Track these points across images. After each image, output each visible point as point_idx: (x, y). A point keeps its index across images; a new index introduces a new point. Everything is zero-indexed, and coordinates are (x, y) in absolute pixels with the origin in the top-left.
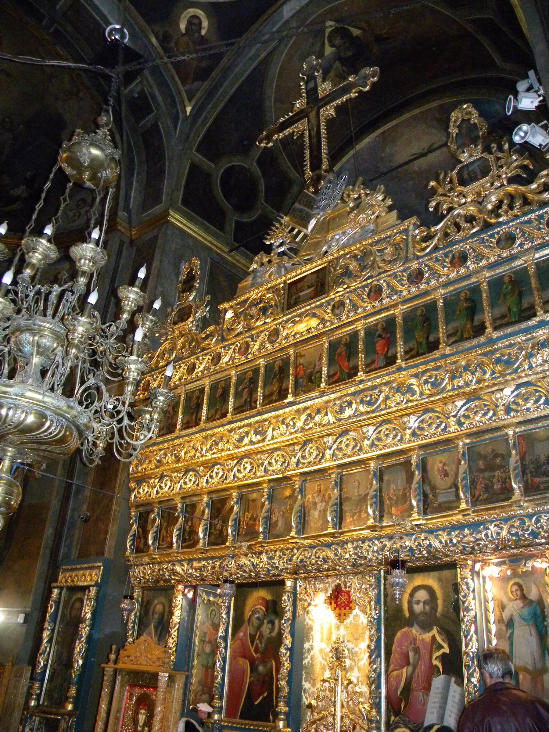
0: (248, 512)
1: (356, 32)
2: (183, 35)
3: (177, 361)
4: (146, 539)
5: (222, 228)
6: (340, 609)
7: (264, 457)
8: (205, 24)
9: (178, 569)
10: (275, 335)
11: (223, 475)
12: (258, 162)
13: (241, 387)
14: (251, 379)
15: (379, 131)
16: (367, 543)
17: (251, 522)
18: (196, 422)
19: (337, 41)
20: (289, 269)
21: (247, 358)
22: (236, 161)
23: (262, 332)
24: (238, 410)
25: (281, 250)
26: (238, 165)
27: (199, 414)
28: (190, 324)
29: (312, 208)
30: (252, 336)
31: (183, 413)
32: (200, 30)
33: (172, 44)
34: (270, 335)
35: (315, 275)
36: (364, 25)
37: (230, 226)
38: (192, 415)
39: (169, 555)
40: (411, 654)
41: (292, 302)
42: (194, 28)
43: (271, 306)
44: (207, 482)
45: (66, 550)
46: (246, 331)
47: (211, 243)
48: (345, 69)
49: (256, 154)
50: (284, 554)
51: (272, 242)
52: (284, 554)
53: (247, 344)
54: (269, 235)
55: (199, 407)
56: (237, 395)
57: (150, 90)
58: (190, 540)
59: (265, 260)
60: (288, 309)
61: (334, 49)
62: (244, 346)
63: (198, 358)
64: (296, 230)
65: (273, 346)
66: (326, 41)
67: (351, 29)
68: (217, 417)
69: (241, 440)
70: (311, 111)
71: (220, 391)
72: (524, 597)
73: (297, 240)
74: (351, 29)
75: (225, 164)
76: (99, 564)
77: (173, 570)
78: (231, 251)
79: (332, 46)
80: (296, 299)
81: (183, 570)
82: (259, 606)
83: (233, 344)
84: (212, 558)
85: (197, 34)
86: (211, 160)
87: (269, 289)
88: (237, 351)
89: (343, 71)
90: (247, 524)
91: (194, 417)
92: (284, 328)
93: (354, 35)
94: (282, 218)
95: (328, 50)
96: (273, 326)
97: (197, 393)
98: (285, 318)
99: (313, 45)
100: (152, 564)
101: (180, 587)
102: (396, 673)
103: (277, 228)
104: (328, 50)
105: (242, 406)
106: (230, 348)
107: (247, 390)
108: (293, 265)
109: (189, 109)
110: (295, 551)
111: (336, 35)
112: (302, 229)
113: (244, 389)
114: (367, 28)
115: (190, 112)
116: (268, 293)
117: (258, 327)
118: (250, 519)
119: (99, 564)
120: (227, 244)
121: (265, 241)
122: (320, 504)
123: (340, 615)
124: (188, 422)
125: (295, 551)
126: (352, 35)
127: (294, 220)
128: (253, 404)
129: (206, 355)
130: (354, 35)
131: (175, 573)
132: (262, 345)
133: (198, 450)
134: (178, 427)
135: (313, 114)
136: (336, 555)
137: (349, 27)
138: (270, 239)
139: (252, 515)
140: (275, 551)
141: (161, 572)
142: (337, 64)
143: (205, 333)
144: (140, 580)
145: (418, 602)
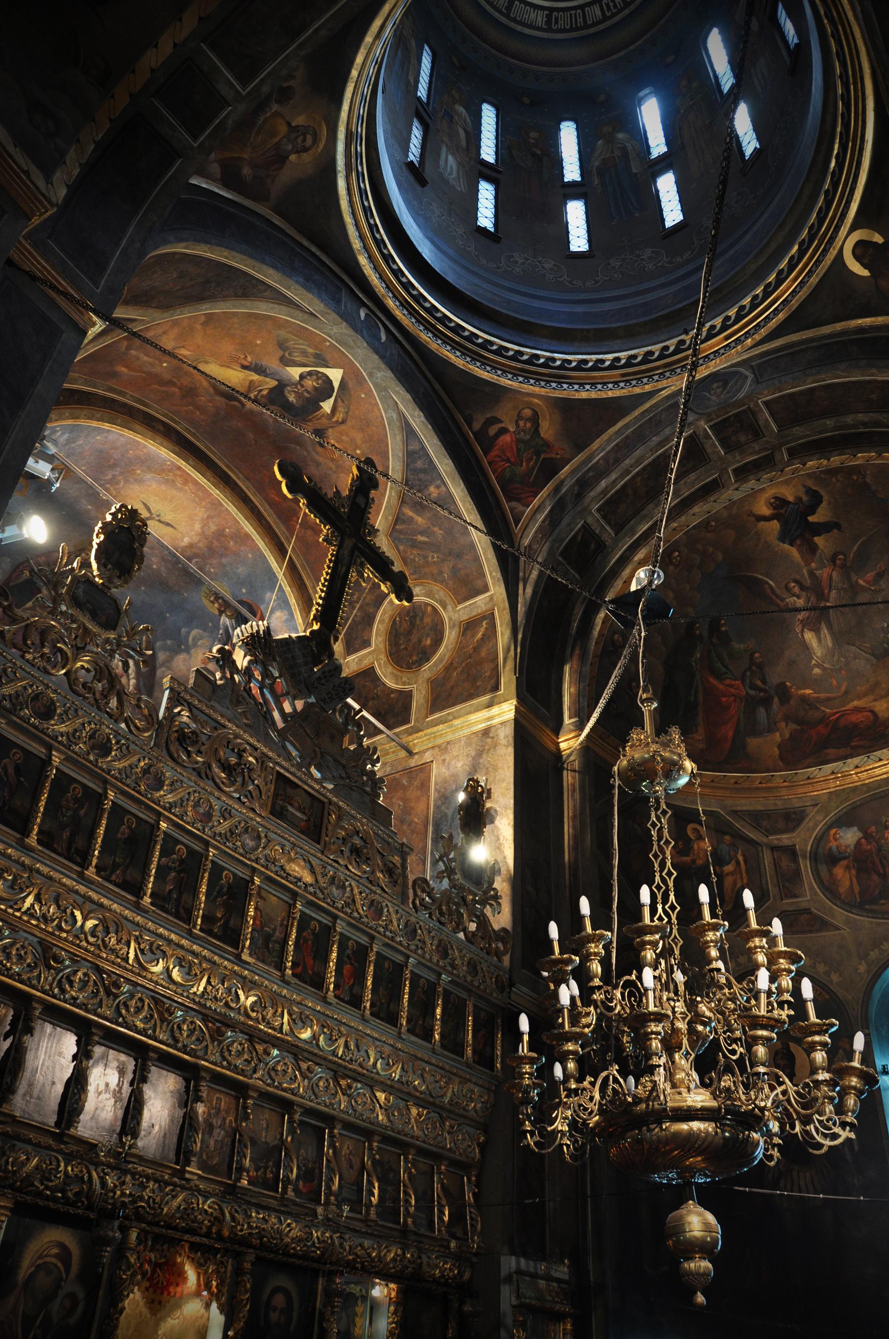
1: (327, 406)
2: (289, 124)
6: (155, 1292)
8: (306, 157)
15: (182, 463)
19: (309, 383)
32: (298, 152)
33: (275, 107)
36: (339, 416)
42: (300, 140)
48: (265, 392)
57: (230, 122)
66: (309, 369)
67: (332, 400)
74: (332, 400)
79: (302, 377)
82: (54, 1260)
85: (290, 147)
89: (261, 391)
95: (295, 372)
99: (304, 353)
104: (295, 372)
111: (320, 382)
114: (335, 419)
122: (218, 1130)
123: (153, 1301)
126: (323, 401)
137: (333, 397)
142: (273, 383)
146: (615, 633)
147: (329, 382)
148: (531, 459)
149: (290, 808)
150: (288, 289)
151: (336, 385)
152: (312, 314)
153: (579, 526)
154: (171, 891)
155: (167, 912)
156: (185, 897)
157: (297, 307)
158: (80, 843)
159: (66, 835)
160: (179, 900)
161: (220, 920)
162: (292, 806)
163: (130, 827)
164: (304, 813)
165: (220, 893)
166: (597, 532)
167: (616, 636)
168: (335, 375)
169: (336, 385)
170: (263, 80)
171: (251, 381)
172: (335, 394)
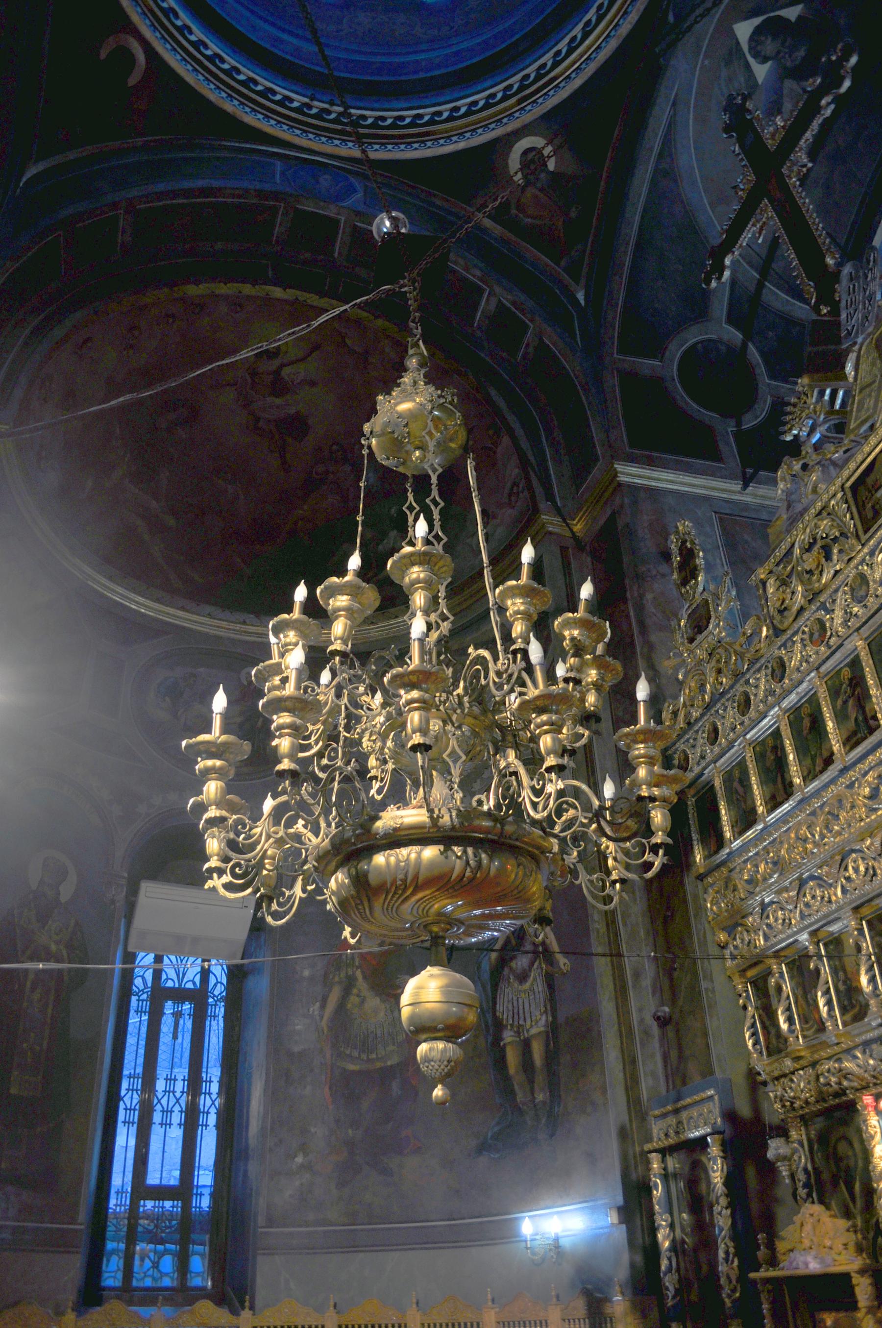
1: (792, 13)
3: (719, 700)
4: (777, 1025)
5: (720, 460)
9: (848, 1065)
10: (861, 586)
11: (867, 869)
12: (729, 321)
13: (839, 702)
14: (851, 680)
18: (786, 793)
19: (769, 46)
20: (840, 462)
21: (829, 647)
22: (693, 336)
23: (836, 591)
24: (851, 741)
25: (817, 437)
26: (698, 343)
27: (786, 776)
28: (716, 630)
29: (839, 342)
30: (823, 606)
31: (762, 783)
34: (852, 590)
37: (729, 448)
39: (825, 1045)
41: (870, 514)
43: (835, 540)
44: (844, 891)
45: (651, 1082)
46: (810, 602)
47: (705, 487)
49: (720, 307)
51: (795, 432)
53: (821, 623)
54: (785, 424)
55: (781, 763)
56: (840, 717)
58: (853, 1006)
59: (797, 466)
60: (866, 532)
61: (769, 64)
62: (816, 627)
63: (747, 682)
64: (828, 392)
65: (865, 606)
66: (751, 60)
68: (818, 769)
71: (807, 723)
73: (837, 406)
75: (676, 350)
76: (711, 1092)
77: (840, 1070)
78: (745, 486)
79: (764, 60)
80: (873, 507)
83: (796, 633)
86: (655, 357)
87: (820, 513)
88: (808, 642)
91: (780, 786)
92: (870, 566)
93: (793, 19)
94: (796, 383)
95: (761, 71)
96: (851, 572)
97: (770, 742)
98: (866, 550)
100: (802, 1069)
101: (868, 1099)
103: (795, 405)
105: (855, 733)
106: (794, 642)
107: (851, 702)
108: (845, 452)
109: (581, 296)
112: (835, 384)
113: (845, 702)
115: (585, 299)
116: (822, 520)
117: (826, 586)
119: (711, 1092)
120: (731, 477)
121: (783, 437)
124: (773, 797)
126: (789, 21)
127: (816, 376)
128: (871, 722)
129: (759, 670)
130: (793, 19)
131: (846, 1075)
132: (846, 612)
133: (807, 838)
134: (760, 809)
138: (791, 429)
141: (822, 1080)
144: (792, 1103)
147: (758, 31)
150: (651, 149)
151: (757, 21)
152: (674, 104)
157: (671, 125)
168: (744, 30)
169: (757, 21)
170: (474, 276)
172: (772, 14)
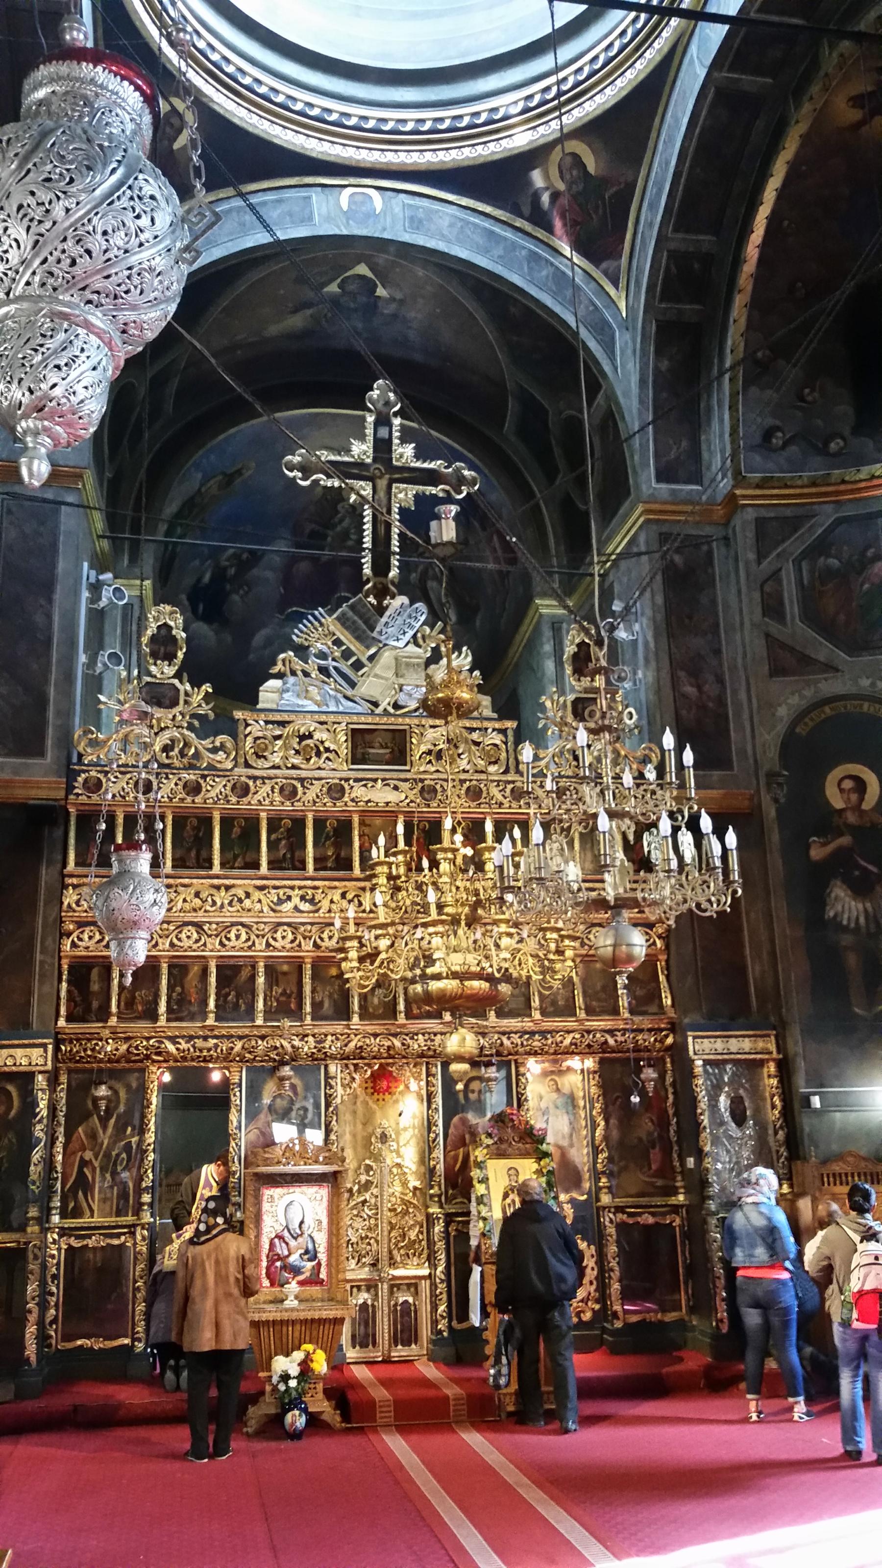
0: (277, 985)
7: (315, 929)
16: (439, 1036)
17: (283, 999)
35: (389, 735)
38: (189, 850)
40: (467, 1137)
50: (337, 1039)
52: (337, 1039)
69: (280, 902)
70: (380, 478)
72: (558, 1090)
81: (178, 1049)
83: (270, 778)
84: (229, 1037)
90: (277, 1000)
102: (452, 1153)
104: (333, 288)
106: (264, 783)
110: (352, 1036)
118: (282, 994)
125: (352, 1036)
135: (382, 483)
136: (403, 1044)
139: (285, 990)
140: (326, 1036)
143: (213, 742)
145: (473, 1091)
146: (755, 352)
148: (597, 207)
149: (372, 751)
151: (370, 274)
153: (664, 261)
154: (284, 854)
155: (285, 869)
156: (297, 854)
158: (204, 854)
159: (193, 854)
160: (292, 858)
161: (331, 857)
162: (373, 747)
163: (240, 827)
164: (387, 748)
165: (328, 838)
166: (691, 249)
167: (759, 354)
168: (362, 269)
169: (370, 274)
171: (311, 316)
